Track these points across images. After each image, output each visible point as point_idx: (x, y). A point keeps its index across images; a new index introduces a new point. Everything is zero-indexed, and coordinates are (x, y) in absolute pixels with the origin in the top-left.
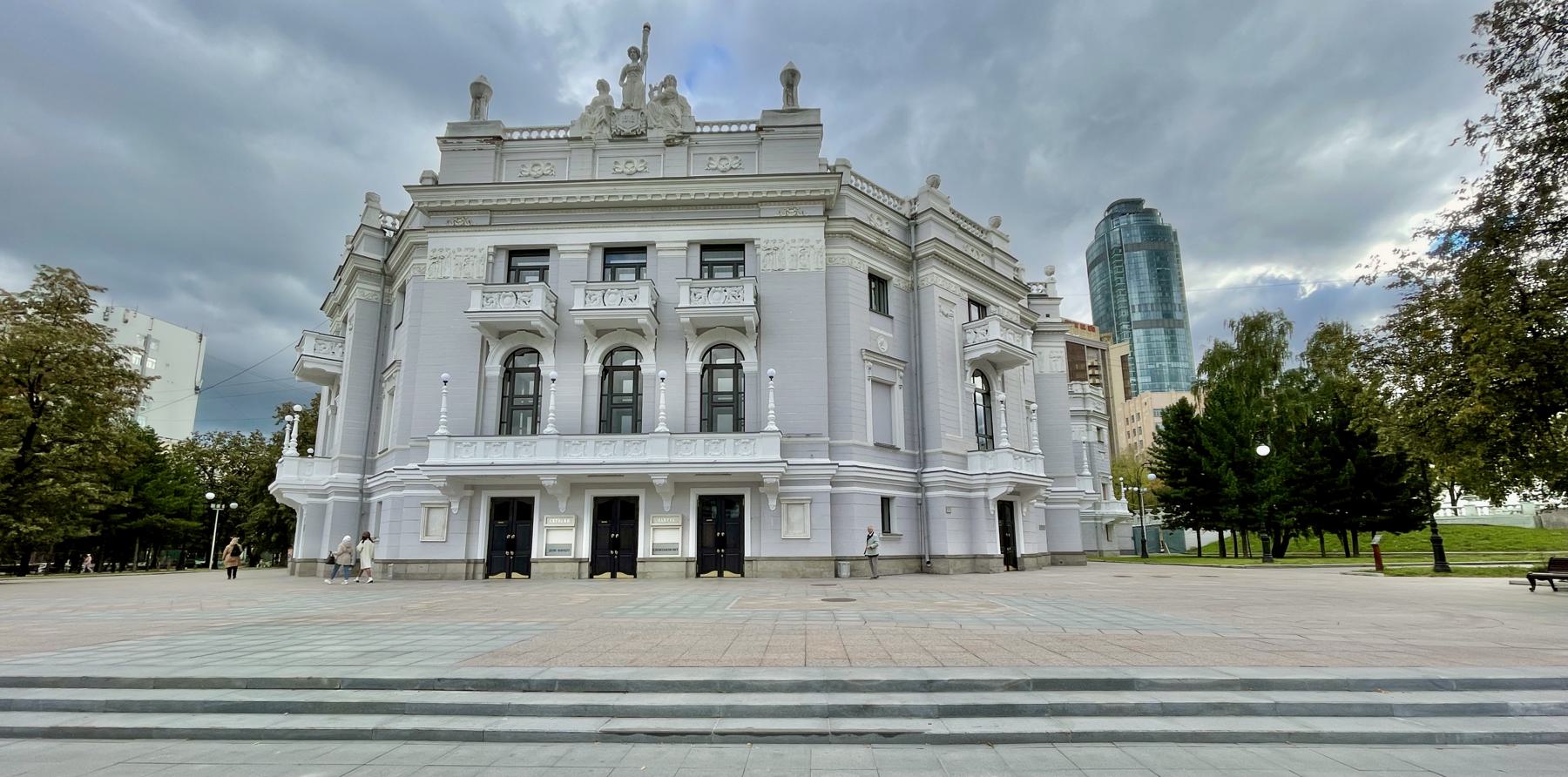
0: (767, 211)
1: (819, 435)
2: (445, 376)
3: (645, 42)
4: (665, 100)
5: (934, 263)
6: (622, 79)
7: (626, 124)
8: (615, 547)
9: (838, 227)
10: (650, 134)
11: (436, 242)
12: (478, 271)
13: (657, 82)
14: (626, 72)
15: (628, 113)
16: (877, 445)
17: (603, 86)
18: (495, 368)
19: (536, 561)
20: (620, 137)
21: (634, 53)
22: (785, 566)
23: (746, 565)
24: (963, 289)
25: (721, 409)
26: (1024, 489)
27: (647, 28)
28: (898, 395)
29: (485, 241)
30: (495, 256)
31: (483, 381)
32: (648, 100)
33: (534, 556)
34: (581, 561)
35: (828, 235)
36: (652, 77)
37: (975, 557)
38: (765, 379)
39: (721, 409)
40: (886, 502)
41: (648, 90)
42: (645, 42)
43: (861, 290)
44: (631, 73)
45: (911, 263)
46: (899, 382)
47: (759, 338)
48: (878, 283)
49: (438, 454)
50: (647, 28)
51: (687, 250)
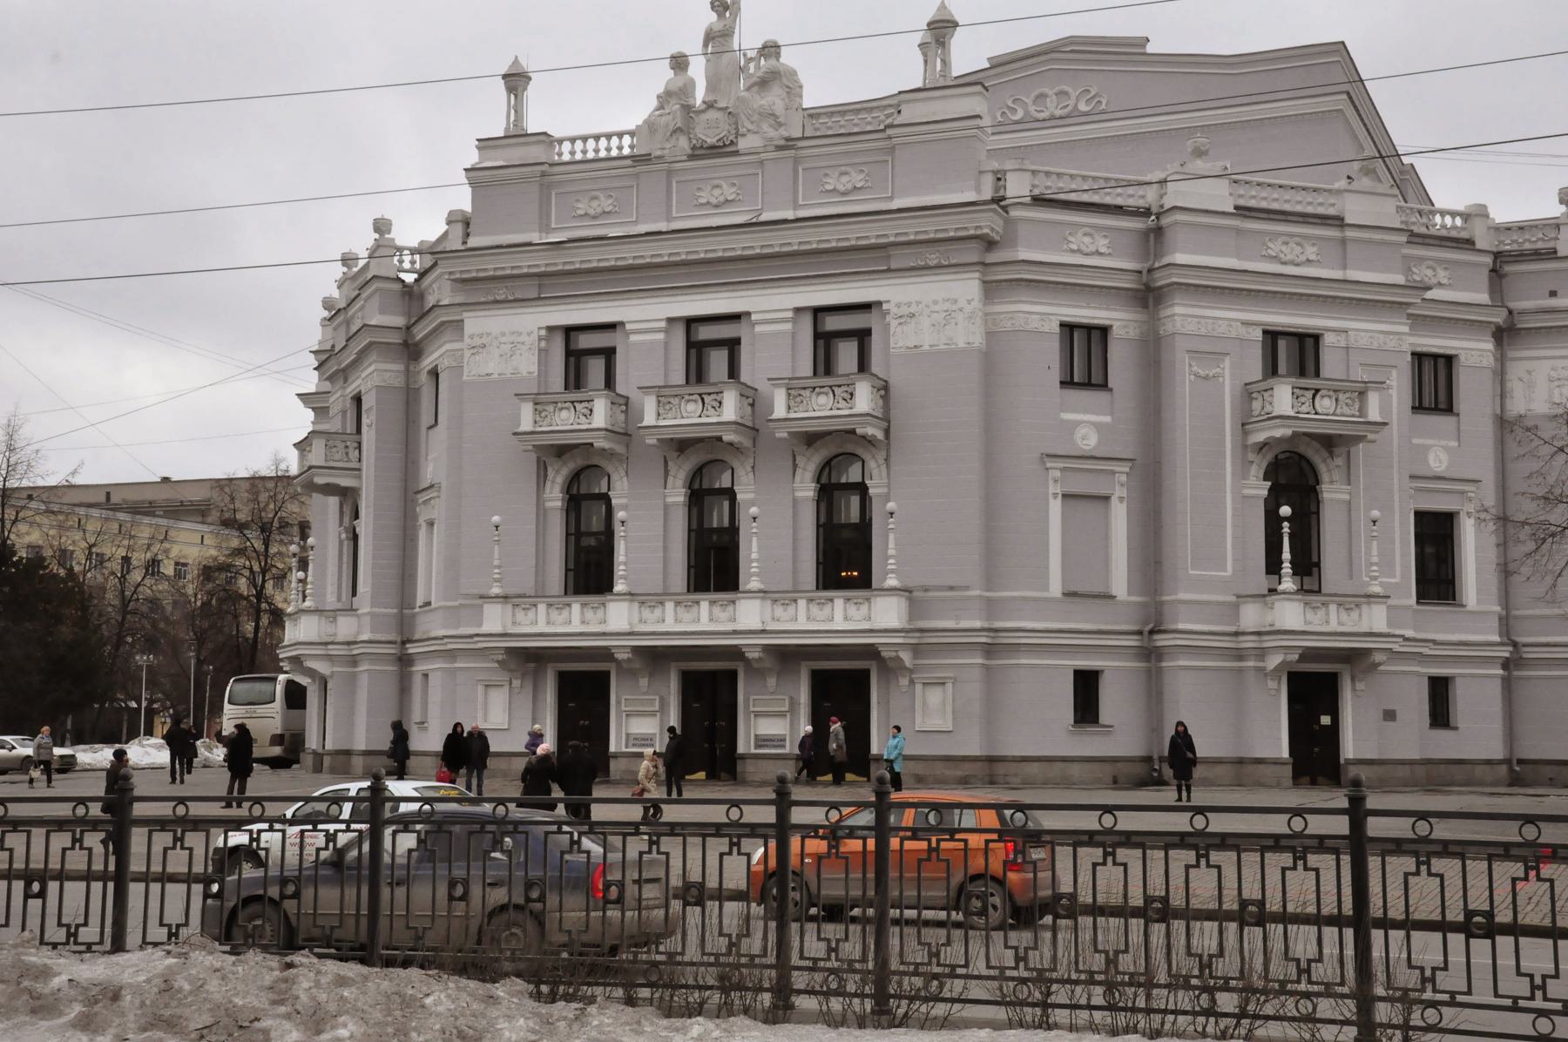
1: (967, 588)
2: (496, 519)
4: (764, 83)
7: (710, 130)
10: (743, 144)
11: (477, 324)
12: (527, 364)
14: (709, 37)
15: (712, 115)
16: (1070, 595)
17: (679, 63)
18: (555, 498)
19: (616, 756)
26: (1355, 658)
29: (535, 320)
30: (547, 339)
33: (612, 749)
35: (991, 290)
37: (1240, 761)
46: (1119, 492)
49: (494, 620)
51: (794, 320)
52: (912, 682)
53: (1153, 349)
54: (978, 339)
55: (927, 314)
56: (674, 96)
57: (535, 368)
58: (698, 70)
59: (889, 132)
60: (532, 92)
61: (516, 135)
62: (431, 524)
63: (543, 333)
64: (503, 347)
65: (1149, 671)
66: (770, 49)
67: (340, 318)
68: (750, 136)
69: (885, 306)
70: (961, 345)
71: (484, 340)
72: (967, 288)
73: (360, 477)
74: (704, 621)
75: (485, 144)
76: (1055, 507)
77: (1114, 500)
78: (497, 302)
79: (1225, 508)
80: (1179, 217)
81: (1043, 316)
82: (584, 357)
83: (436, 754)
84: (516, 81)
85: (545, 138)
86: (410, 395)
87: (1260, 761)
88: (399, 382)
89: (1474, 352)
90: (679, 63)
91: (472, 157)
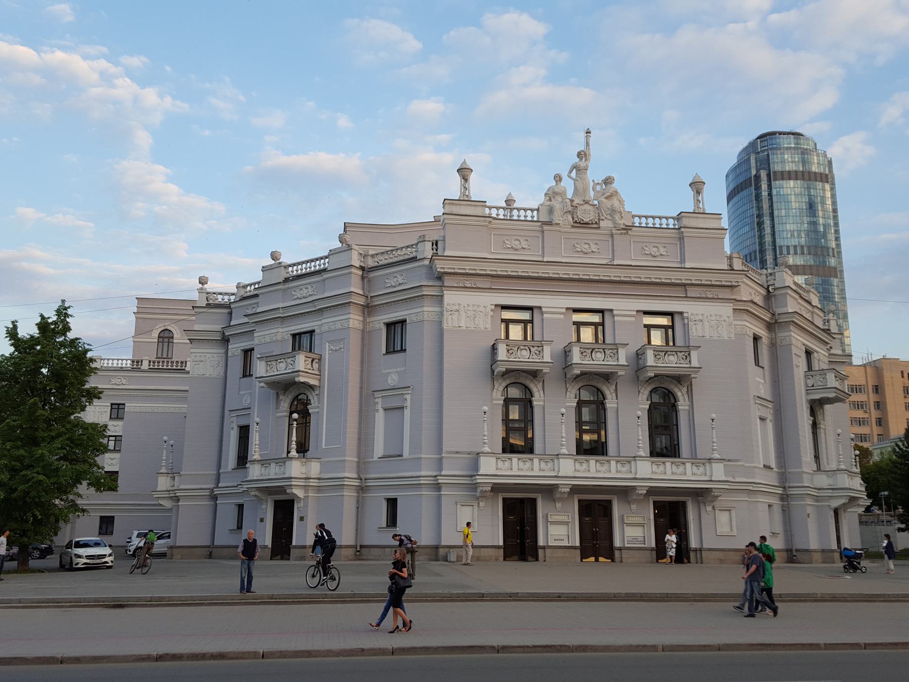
0: (692, 292)
1: (737, 461)
3: (587, 144)
5: (792, 328)
6: (571, 172)
8: (596, 539)
10: (602, 224)
13: (600, 178)
14: (575, 167)
15: (587, 207)
17: (558, 178)
20: (580, 224)
22: (720, 555)
23: (541, 552)
25: (665, 439)
27: (588, 132)
28: (770, 426)
32: (592, 193)
36: (595, 175)
39: (665, 439)
41: (592, 184)
42: (587, 144)
44: (579, 170)
50: (588, 132)
52: (713, 508)
54: (732, 336)
56: (551, 195)
57: (489, 326)
58: (568, 186)
59: (682, 230)
61: (465, 200)
63: (493, 307)
65: (783, 506)
66: (608, 181)
68: (606, 221)
69: (685, 315)
70: (726, 338)
71: (457, 307)
74: (594, 472)
77: (768, 421)
78: (466, 287)
83: (652, 549)
84: (464, 172)
86: (366, 335)
87: (807, 551)
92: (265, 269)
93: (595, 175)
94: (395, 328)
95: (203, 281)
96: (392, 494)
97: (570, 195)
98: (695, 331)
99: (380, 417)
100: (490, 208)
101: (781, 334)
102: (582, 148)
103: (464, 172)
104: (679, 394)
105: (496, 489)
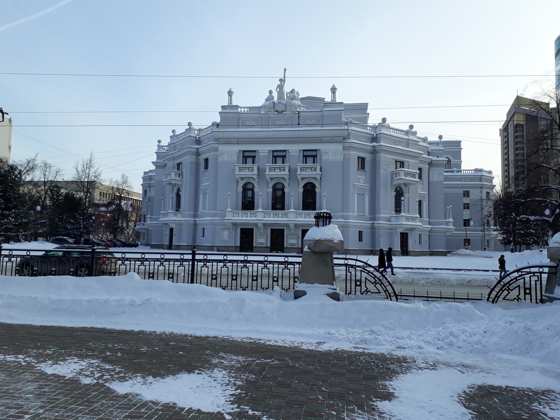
2: (229, 193)
9: (346, 145)
11: (222, 148)
12: (234, 158)
13: (289, 91)
14: (278, 86)
17: (271, 92)
18: (240, 189)
21: (281, 80)
24: (393, 159)
26: (412, 229)
27: (285, 70)
28: (367, 198)
30: (239, 153)
31: (237, 192)
34: (268, 247)
35: (344, 148)
36: (287, 89)
38: (322, 196)
40: (360, 233)
43: (354, 164)
44: (280, 87)
45: (374, 152)
46: (367, 193)
47: (321, 182)
48: (362, 161)
50: (285, 70)
53: (375, 163)
55: (330, 152)
56: (270, 98)
57: (236, 159)
58: (275, 95)
60: (233, 96)
61: (231, 106)
62: (205, 194)
64: (229, 153)
66: (293, 91)
67: (173, 145)
72: (339, 147)
73: (183, 182)
74: (277, 218)
75: (223, 107)
76: (356, 195)
77: (366, 195)
79: (387, 198)
80: (382, 135)
81: (354, 155)
82: (248, 157)
84: (230, 93)
85: (237, 107)
86: (197, 164)
88: (195, 160)
89: (425, 167)
90: (271, 92)
91: (220, 110)
92: (171, 137)
93: (287, 89)
94: (206, 160)
95: (159, 141)
96: (203, 227)
97: (275, 99)
98: (324, 158)
99: (201, 196)
100: (241, 108)
101: (377, 155)
102: (282, 77)
103: (230, 93)
104: (316, 185)
105: (235, 225)
